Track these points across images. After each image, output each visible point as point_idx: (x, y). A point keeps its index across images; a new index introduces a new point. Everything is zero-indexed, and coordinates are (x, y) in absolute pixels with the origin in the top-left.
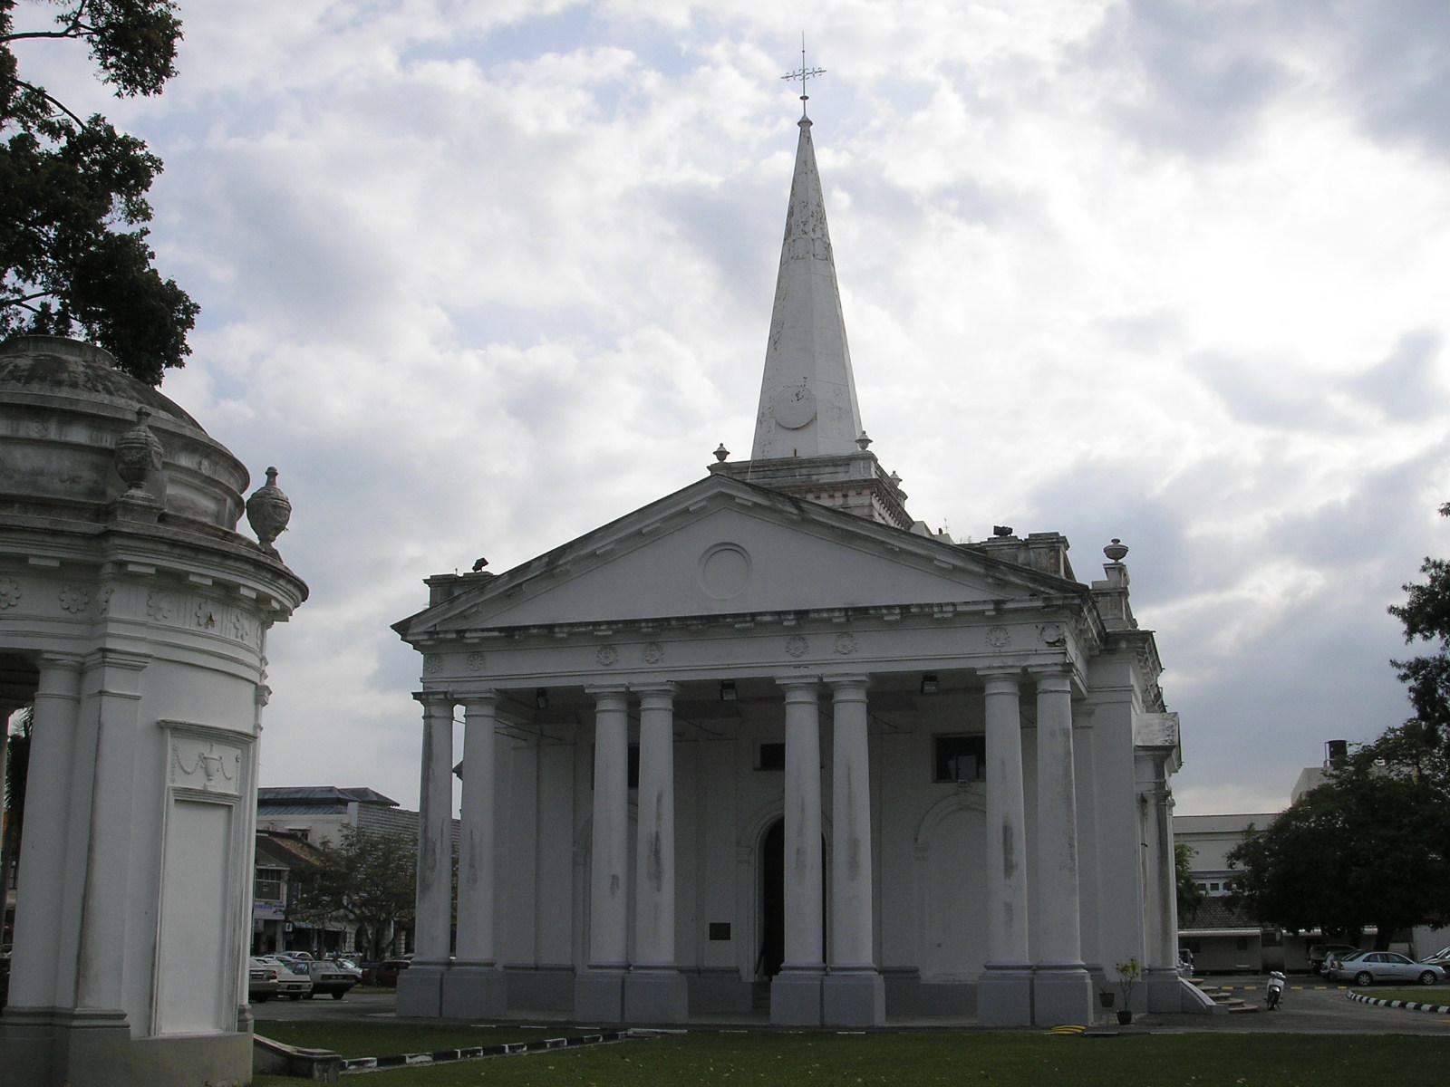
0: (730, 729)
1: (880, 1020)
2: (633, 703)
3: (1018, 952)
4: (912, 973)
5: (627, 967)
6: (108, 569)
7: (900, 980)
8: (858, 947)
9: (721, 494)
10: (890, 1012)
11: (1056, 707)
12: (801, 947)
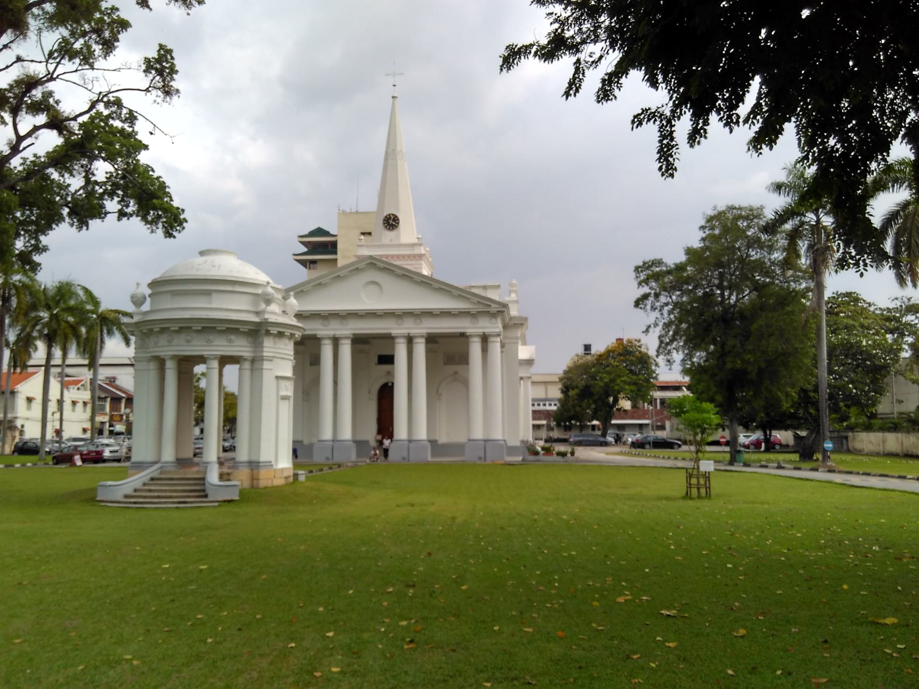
0: (374, 352)
1: (429, 459)
2: (336, 341)
3: (478, 433)
4: (436, 441)
5: (333, 441)
6: (263, 332)
7: (433, 442)
8: (422, 433)
9: (371, 263)
10: (433, 455)
11: (495, 347)
12: (401, 431)
